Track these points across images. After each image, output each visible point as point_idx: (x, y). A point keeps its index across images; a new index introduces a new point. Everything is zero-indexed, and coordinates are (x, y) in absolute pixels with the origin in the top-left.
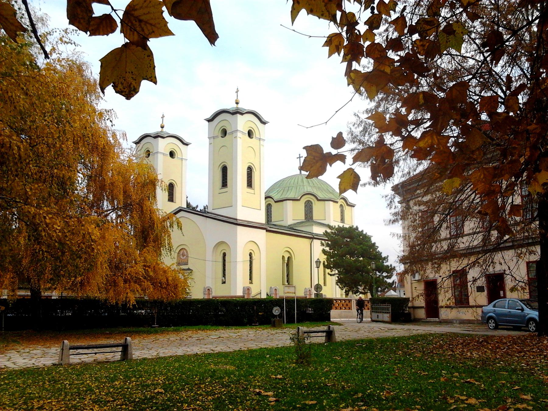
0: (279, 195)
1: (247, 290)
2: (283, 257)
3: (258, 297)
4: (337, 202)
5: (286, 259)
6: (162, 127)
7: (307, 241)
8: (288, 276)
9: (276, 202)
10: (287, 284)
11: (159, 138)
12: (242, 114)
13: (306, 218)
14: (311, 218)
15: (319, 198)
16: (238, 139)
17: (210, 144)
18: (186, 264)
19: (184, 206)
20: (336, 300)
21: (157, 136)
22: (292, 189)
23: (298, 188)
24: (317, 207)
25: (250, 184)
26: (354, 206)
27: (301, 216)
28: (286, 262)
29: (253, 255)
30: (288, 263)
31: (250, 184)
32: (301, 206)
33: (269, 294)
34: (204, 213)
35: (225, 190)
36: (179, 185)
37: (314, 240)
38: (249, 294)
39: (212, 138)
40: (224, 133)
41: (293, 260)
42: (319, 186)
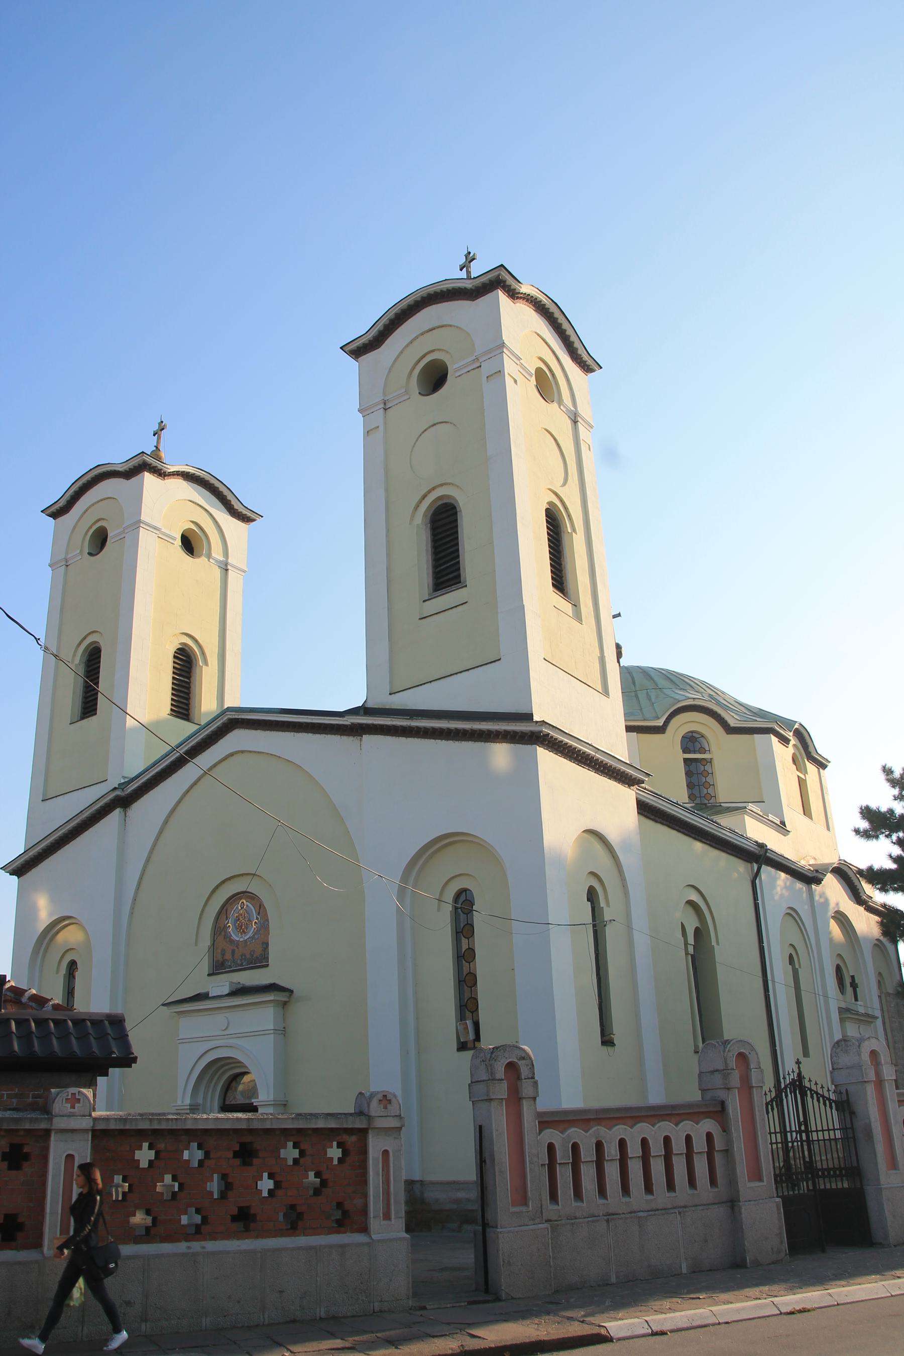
12: (513, 294)
15: (732, 723)
16: (509, 382)
17: (368, 433)
18: (260, 961)
21: (136, 469)
23: (642, 695)
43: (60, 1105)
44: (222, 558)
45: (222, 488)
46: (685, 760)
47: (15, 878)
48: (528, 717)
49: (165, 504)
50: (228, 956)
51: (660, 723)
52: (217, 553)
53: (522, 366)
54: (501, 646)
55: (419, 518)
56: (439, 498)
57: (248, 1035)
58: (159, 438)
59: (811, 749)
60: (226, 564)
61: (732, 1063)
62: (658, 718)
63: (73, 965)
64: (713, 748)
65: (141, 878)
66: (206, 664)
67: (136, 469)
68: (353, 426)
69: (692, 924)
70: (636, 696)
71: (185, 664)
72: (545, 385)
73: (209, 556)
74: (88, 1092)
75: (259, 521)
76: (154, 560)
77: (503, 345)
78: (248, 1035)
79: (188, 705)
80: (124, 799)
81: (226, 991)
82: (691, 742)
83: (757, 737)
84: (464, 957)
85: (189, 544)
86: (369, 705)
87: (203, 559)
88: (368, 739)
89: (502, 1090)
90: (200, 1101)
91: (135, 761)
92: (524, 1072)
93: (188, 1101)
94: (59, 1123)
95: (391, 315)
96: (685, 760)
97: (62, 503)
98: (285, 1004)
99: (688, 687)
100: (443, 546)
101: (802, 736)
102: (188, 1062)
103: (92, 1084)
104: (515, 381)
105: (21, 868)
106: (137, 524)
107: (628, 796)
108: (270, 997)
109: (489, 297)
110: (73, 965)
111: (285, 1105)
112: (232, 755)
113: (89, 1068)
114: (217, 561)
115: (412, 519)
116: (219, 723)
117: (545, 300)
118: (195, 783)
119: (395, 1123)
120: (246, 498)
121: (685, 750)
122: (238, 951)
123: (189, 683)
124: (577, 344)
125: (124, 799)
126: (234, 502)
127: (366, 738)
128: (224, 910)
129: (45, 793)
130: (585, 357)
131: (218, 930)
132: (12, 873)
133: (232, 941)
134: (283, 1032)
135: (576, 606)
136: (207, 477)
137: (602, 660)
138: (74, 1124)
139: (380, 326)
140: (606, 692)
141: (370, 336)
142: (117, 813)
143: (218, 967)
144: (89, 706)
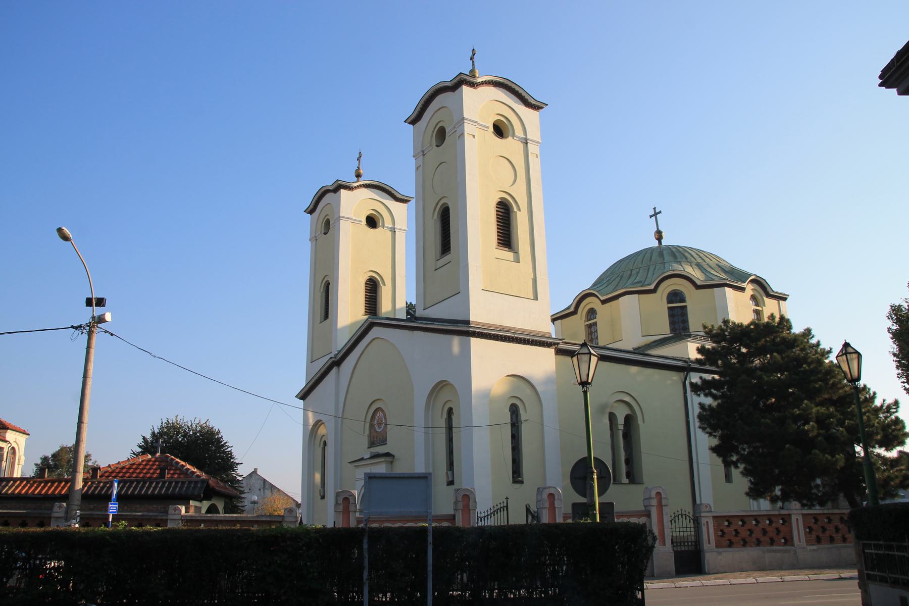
0: (612, 287)
2: (612, 417)
4: (742, 289)
5: (621, 420)
8: (628, 462)
10: (627, 481)
11: (342, 191)
12: (473, 85)
13: (673, 330)
14: (686, 328)
15: (699, 283)
16: (467, 138)
17: (417, 169)
18: (384, 442)
21: (338, 187)
22: (638, 273)
24: (694, 302)
25: (506, 238)
26: (785, 299)
27: (664, 329)
28: (621, 427)
29: (522, 411)
30: (627, 431)
31: (506, 238)
32: (658, 304)
33: (534, 508)
35: (447, 258)
36: (388, 282)
37: (692, 374)
39: (421, 153)
40: (441, 135)
41: (640, 422)
42: (699, 260)
43: (171, 511)
45: (388, 188)
46: (669, 308)
48: (467, 322)
51: (652, 287)
52: (388, 224)
59: (769, 290)
61: (460, 499)
62: (650, 284)
64: (687, 299)
67: (338, 187)
71: (373, 287)
72: (499, 130)
73: (383, 226)
77: (463, 119)
80: (337, 363)
82: (675, 296)
83: (715, 289)
84: (450, 440)
85: (372, 222)
89: (341, 508)
92: (351, 501)
94: (170, 517)
95: (422, 102)
96: (669, 308)
97: (311, 207)
98: (392, 462)
100: (443, 232)
101: (759, 283)
106: (339, 218)
107: (552, 351)
108: (382, 459)
112: (374, 339)
117: (498, 79)
119: (294, 520)
121: (669, 302)
124: (527, 97)
125: (337, 363)
126: (396, 194)
127: (415, 332)
130: (534, 102)
131: (372, 426)
132: (301, 399)
135: (516, 253)
136: (378, 184)
138: (175, 517)
140: (536, 298)
142: (335, 369)
143: (372, 444)
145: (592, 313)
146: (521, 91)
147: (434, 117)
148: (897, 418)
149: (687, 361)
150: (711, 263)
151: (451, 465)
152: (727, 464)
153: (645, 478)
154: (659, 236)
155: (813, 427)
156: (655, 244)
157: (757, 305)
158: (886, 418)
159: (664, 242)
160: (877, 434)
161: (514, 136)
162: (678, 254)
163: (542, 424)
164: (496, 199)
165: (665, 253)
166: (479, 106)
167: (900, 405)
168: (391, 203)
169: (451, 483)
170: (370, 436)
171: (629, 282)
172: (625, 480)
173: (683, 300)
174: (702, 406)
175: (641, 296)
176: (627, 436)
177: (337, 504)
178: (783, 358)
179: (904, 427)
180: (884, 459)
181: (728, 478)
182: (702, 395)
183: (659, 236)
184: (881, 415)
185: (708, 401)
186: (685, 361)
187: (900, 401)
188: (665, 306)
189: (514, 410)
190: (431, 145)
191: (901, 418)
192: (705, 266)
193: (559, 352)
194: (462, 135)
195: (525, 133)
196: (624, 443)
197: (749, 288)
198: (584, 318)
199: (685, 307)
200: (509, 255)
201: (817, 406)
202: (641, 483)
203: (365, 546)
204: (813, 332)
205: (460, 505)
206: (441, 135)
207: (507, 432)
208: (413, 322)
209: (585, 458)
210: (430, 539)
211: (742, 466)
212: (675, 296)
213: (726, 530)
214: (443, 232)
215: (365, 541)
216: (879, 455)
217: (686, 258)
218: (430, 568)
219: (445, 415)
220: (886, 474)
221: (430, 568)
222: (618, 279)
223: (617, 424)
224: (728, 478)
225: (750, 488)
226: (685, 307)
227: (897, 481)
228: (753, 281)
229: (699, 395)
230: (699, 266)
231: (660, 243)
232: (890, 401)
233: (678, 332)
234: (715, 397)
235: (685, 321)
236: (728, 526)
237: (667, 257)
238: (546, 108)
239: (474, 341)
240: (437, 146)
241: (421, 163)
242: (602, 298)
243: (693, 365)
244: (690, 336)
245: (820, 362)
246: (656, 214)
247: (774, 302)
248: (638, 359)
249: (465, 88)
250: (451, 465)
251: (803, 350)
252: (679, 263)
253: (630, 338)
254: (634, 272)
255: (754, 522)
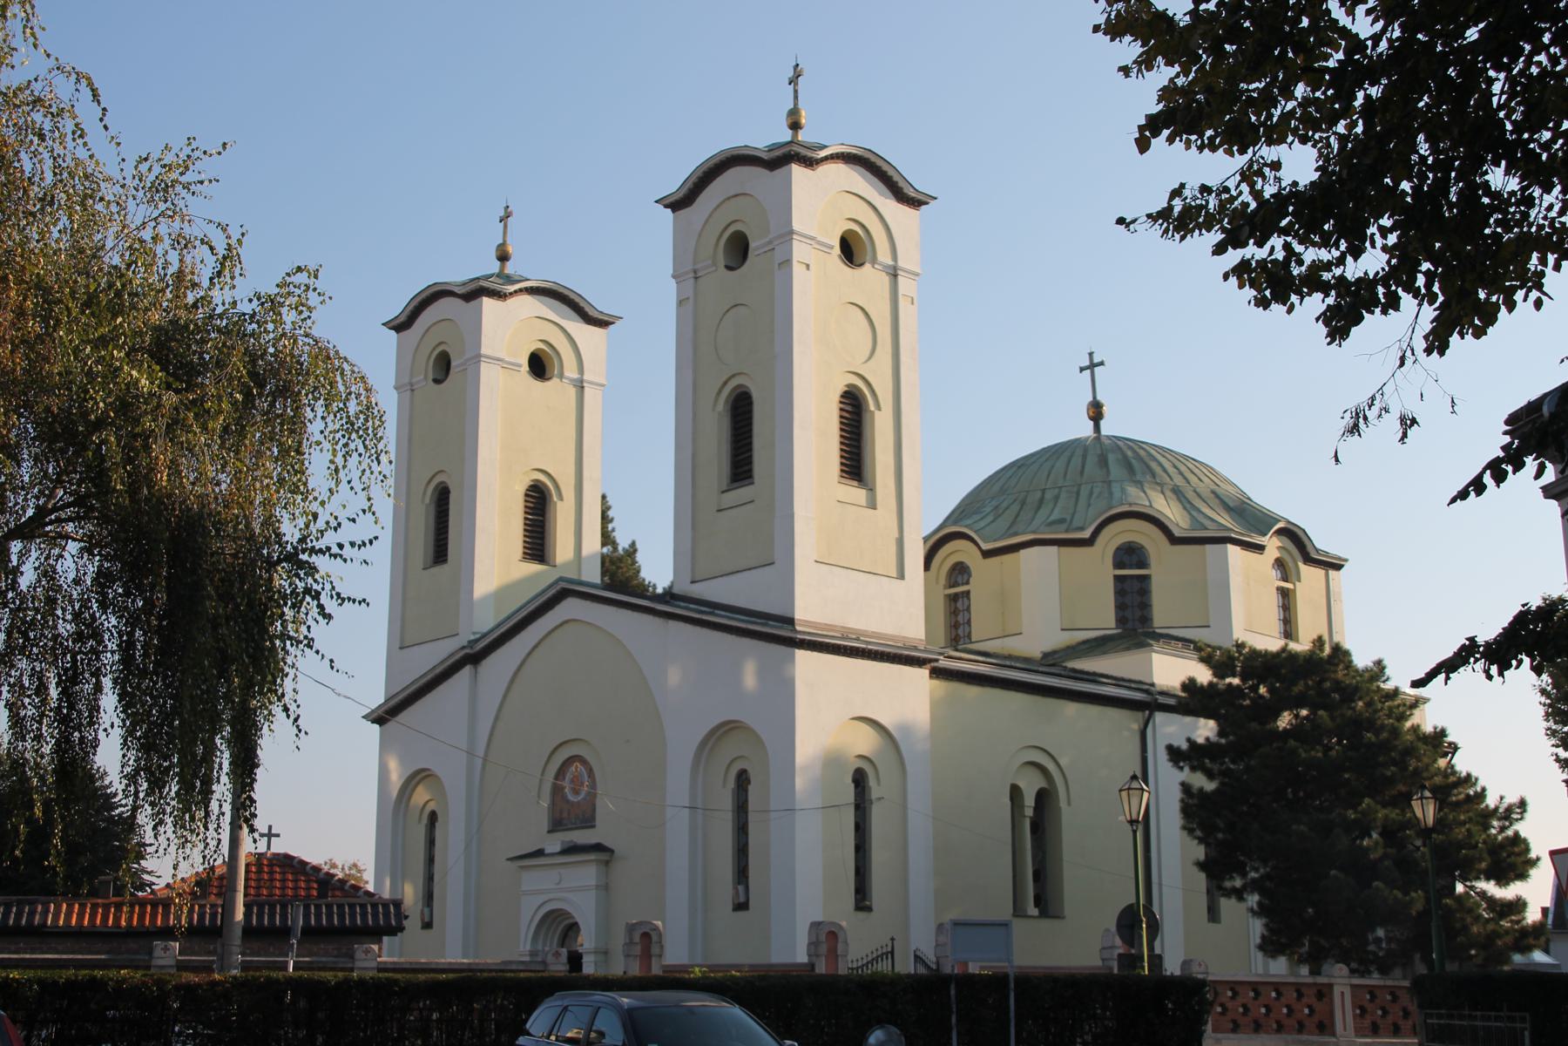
0: (1003, 523)
1: (827, 937)
2: (1015, 792)
3: (884, 967)
4: (1260, 548)
5: (1029, 801)
6: (503, 257)
7: (1129, 722)
8: (1038, 876)
9: (987, 554)
10: (1034, 911)
11: (486, 301)
12: (810, 163)
13: (1121, 621)
14: (1146, 619)
15: (1177, 533)
16: (797, 269)
17: (680, 303)
18: (588, 822)
19: (593, 574)
20: (1234, 986)
21: (475, 292)
22: (1057, 498)
23: (1084, 492)
25: (855, 465)
26: (1338, 567)
27: (1104, 619)
28: (1029, 812)
29: (872, 782)
30: (1038, 819)
32: (1096, 570)
34: (671, 606)
35: (743, 493)
37: (1159, 717)
38: (833, 955)
39: (688, 274)
40: (738, 249)
41: (1063, 804)
42: (1178, 481)
43: (359, 955)
44: (576, 376)
45: (572, 296)
46: (1117, 578)
47: (376, 727)
48: (790, 621)
49: (507, 328)
50: (565, 815)
51: (1086, 534)
52: (571, 372)
53: (820, 243)
54: (773, 553)
55: (721, 406)
56: (740, 386)
57: (575, 893)
58: (505, 226)
60: (582, 381)
61: (823, 938)
62: (1082, 529)
63: (433, 817)
64: (1153, 562)
65: (491, 734)
66: (561, 498)
67: (475, 292)
68: (669, 291)
69: (1030, 786)
70: (1078, 493)
71: (538, 501)
72: (851, 250)
73: (561, 376)
74: (375, 947)
75: (618, 323)
76: (500, 391)
77: (792, 232)
78: (575, 893)
79: (542, 545)
80: (474, 656)
81: (558, 849)
82: (1130, 555)
83: (1208, 547)
84: (741, 829)
85: (539, 366)
86: (676, 590)
87: (555, 381)
88: (672, 624)
89: (638, 950)
90: (540, 947)
91: (485, 621)
92: (655, 938)
93: (528, 947)
94: (358, 964)
95: (699, 173)
96: (1117, 578)
97: (402, 319)
98: (607, 863)
99: (1148, 477)
100: (736, 438)
101: (1294, 536)
102: (529, 912)
103: (380, 942)
104: (808, 266)
105: (381, 718)
106: (477, 358)
108: (592, 856)
109: (784, 169)
110: (433, 817)
111: (606, 953)
113: (375, 934)
114: (572, 380)
115: (715, 404)
116: (552, 592)
117: (854, 151)
118: (536, 646)
120: (600, 303)
122: (571, 812)
123: (543, 522)
124: (901, 184)
125: (474, 656)
126: (587, 309)
128: (560, 773)
129: (402, 641)
130: (912, 194)
131: (557, 790)
133: (568, 801)
134: (605, 888)
135: (871, 490)
136: (555, 287)
137: (900, 543)
138: (366, 964)
139: (689, 184)
140: (901, 576)
141: (681, 195)
142: (467, 670)
143: (557, 825)
144: (440, 553)
145: (960, 572)
146: (891, 172)
147: (728, 215)
148: (1516, 834)
149: (1147, 688)
150: (1201, 488)
151: (741, 874)
152: (1216, 889)
153: (1068, 909)
154: (1096, 412)
155: (1377, 843)
156: (1085, 429)
157: (1285, 579)
158: (1502, 829)
159: (1107, 428)
160: (1481, 860)
161: (874, 261)
162: (1135, 460)
163: (904, 807)
164: (840, 388)
165: (1111, 457)
166: (820, 202)
167: (1529, 808)
168: (578, 328)
169: (741, 906)
170: (553, 803)
171: (1043, 513)
172: (1033, 910)
173: (1143, 564)
174: (1186, 788)
175: (1065, 550)
176: (1037, 827)
177: (630, 943)
178: (1332, 718)
179: (1528, 850)
180: (1492, 902)
181: (1213, 914)
182: (1187, 769)
183: (1096, 412)
184: (1495, 823)
185: (1200, 781)
186: (1147, 692)
187: (1528, 800)
188: (1108, 573)
189: (859, 779)
190: (714, 264)
191: (1523, 834)
192: (1190, 495)
193: (937, 673)
194: (787, 262)
195: (895, 258)
196: (1033, 840)
197: (1273, 545)
198: (943, 581)
199: (1146, 578)
200: (857, 494)
201: (1384, 807)
202: (1059, 916)
203: (953, 992)
204: (1388, 672)
205: (824, 949)
206: (738, 249)
207: (849, 817)
208: (667, 603)
209: (1130, 907)
210: (1012, 985)
211: (1253, 899)
212: (1130, 555)
213: (1229, 1005)
214: (736, 438)
215: (953, 986)
216: (1483, 894)
217: (1154, 475)
218: (1012, 1014)
219: (731, 783)
220: (1490, 927)
221: (1012, 1014)
222: (1016, 507)
223: (1022, 806)
224: (1213, 914)
225: (1263, 937)
226: (1146, 578)
227: (1509, 939)
228: (1280, 532)
229: (1181, 769)
230: (1178, 493)
231: (1097, 428)
232: (1512, 798)
233: (1129, 625)
234: (1210, 775)
235: (1145, 606)
236: (1233, 998)
237: (1116, 471)
238: (932, 203)
239: (801, 655)
240: (729, 268)
241: (690, 293)
242: (985, 547)
243: (1161, 699)
244: (1158, 637)
245: (1395, 732)
246: (1092, 366)
247: (1319, 573)
248: (1053, 679)
249: (797, 170)
250: (741, 874)
251: (1369, 704)
252: (1140, 484)
253: (1039, 633)
254: (1048, 495)
255: (1274, 994)
